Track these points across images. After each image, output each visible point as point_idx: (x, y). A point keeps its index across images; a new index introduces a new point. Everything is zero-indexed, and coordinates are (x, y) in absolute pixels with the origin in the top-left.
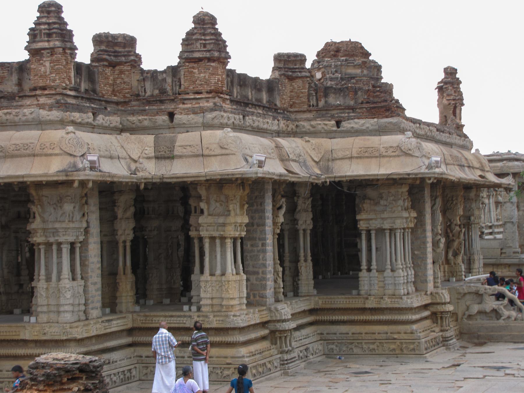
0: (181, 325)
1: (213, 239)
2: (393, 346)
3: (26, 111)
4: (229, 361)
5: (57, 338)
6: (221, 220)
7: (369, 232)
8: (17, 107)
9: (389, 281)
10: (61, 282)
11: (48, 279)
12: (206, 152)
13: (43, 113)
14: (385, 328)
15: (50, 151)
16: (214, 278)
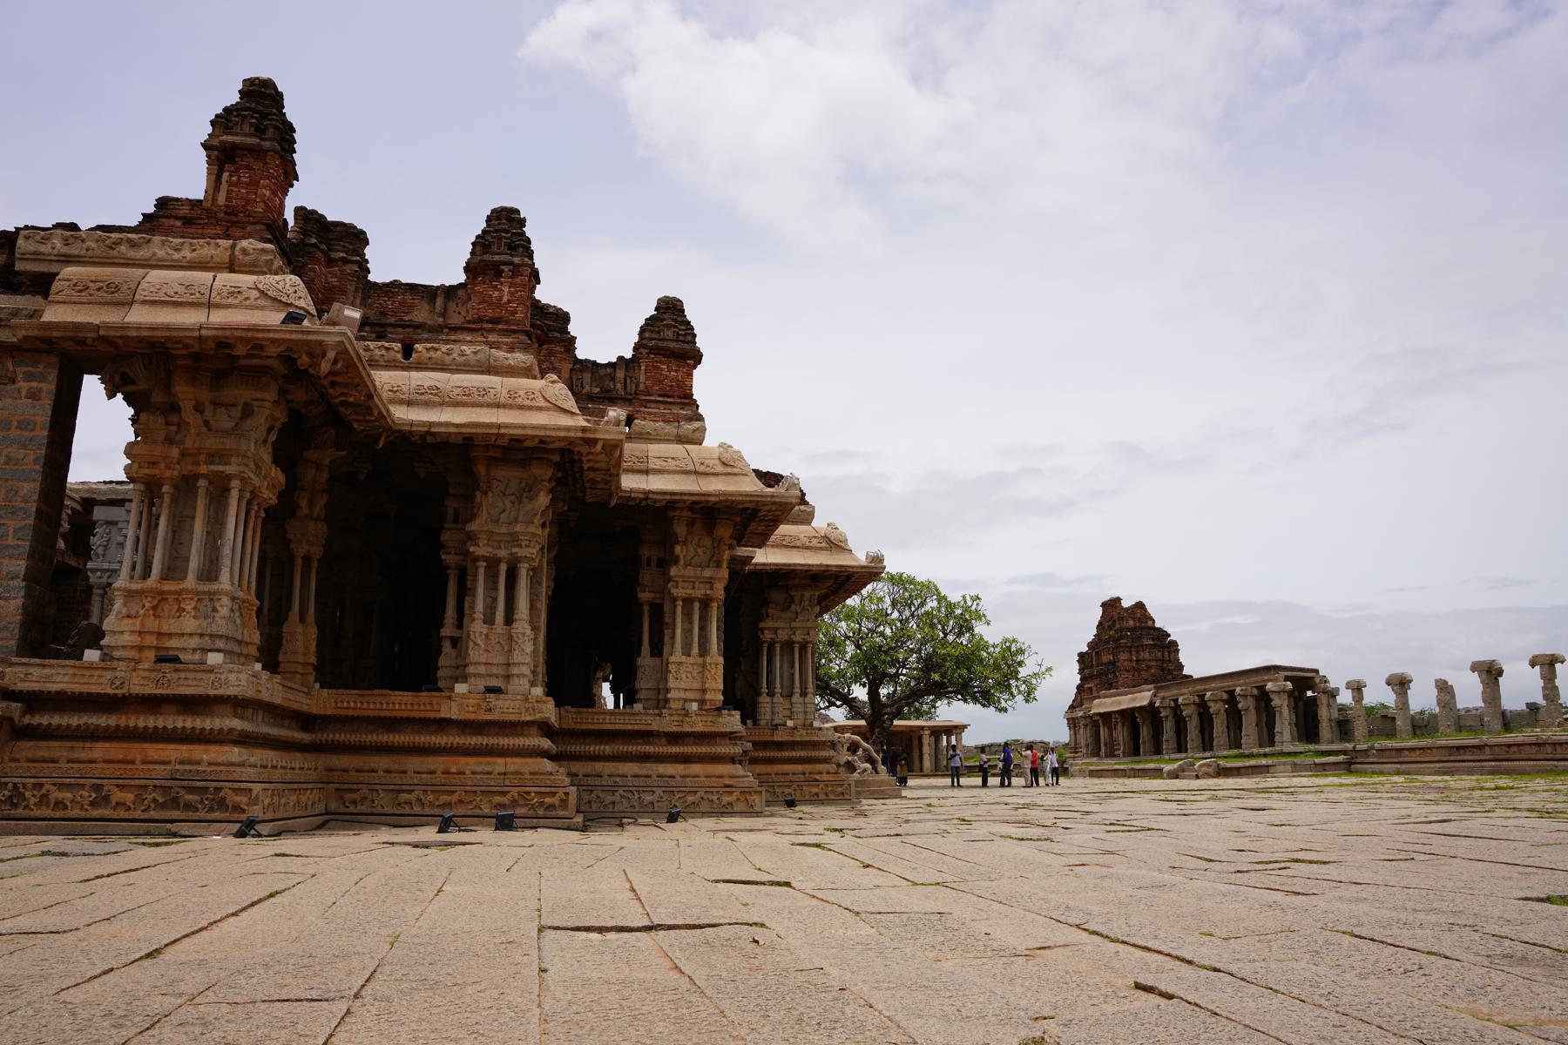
0: (643, 728)
1: (688, 601)
2: (815, 790)
3: (468, 349)
4: (728, 782)
5: (512, 718)
6: (707, 573)
7: (771, 646)
8: (447, 342)
9: (798, 708)
10: (515, 625)
11: (489, 620)
12: (702, 469)
13: (500, 354)
14: (800, 768)
15: (527, 403)
16: (690, 660)
